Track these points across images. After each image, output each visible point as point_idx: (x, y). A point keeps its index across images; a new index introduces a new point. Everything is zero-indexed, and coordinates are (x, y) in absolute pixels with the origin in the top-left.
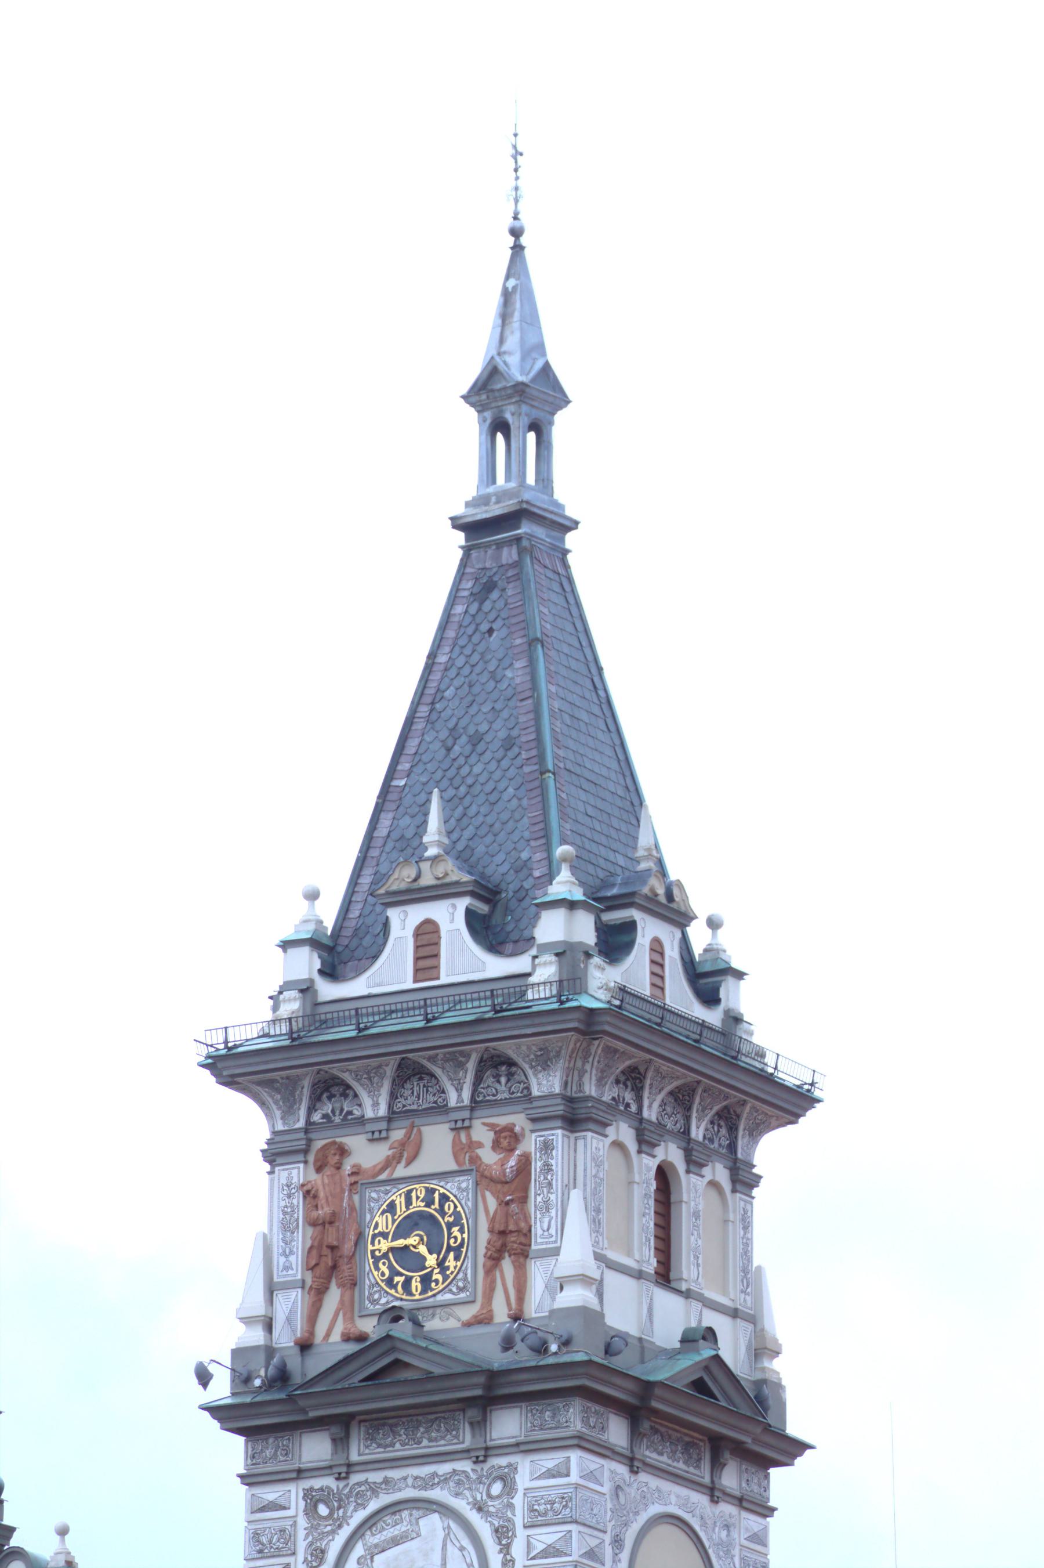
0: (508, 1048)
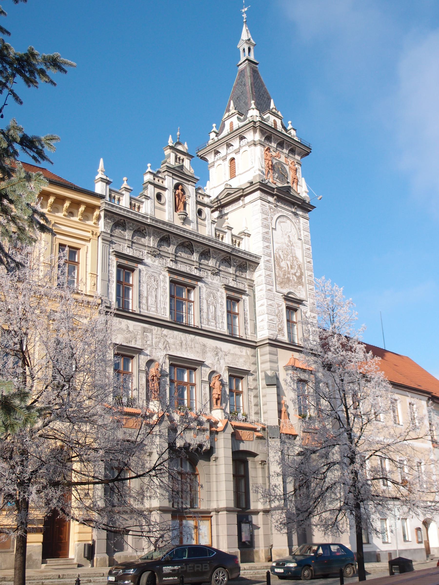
0: (297, 150)
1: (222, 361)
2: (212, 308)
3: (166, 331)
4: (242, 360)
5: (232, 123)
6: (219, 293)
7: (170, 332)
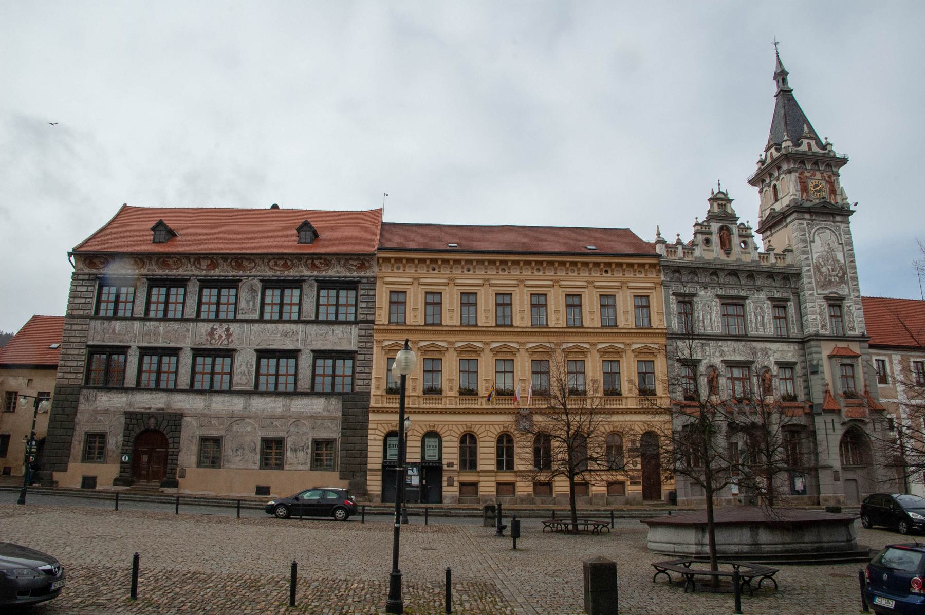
1: (771, 358)
2: (760, 318)
3: (720, 343)
4: (790, 354)
5: (771, 154)
6: (765, 305)
7: (724, 343)
